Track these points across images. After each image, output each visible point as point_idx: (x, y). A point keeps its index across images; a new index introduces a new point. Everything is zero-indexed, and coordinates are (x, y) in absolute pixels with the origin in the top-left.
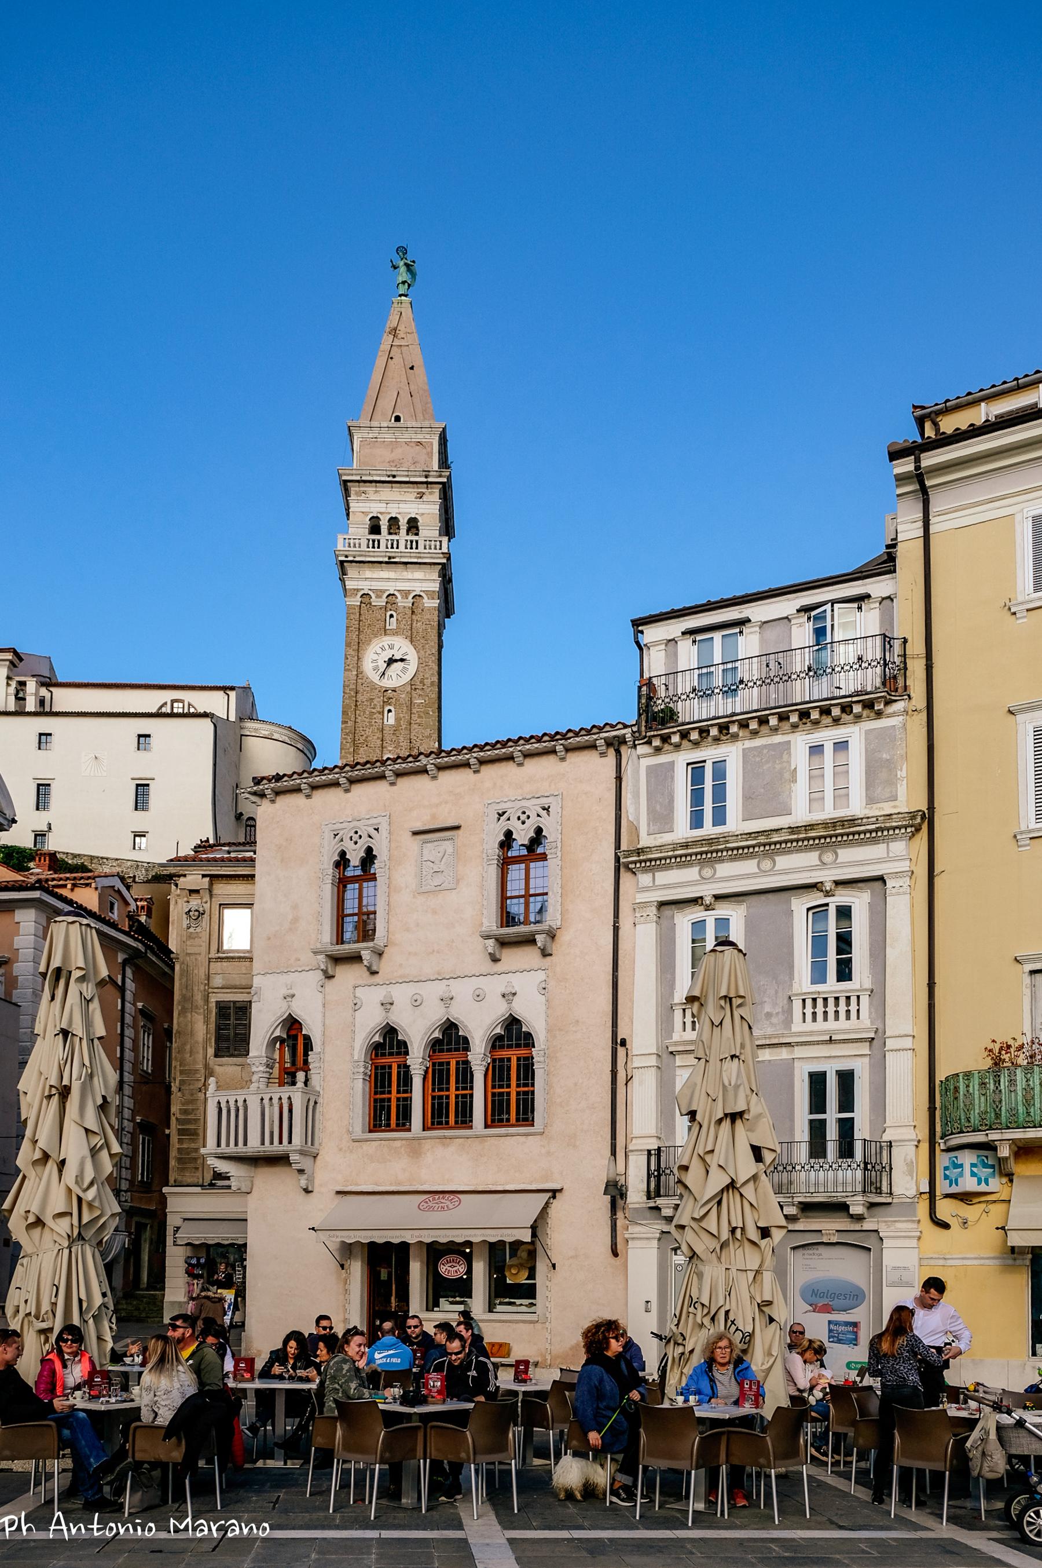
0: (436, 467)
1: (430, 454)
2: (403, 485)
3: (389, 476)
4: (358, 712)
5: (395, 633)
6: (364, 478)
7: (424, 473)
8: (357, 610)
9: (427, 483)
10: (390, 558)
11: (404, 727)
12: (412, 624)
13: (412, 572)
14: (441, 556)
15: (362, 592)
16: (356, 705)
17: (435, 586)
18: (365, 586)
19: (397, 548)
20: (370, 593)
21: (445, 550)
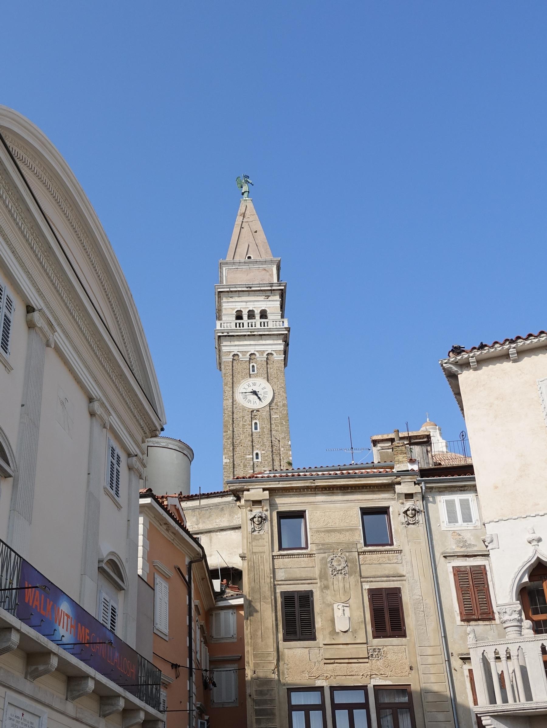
0: (275, 281)
1: (272, 275)
2: (256, 292)
3: (247, 288)
4: (234, 425)
5: (256, 376)
6: (232, 289)
7: (270, 285)
8: (231, 364)
9: (271, 290)
10: (251, 332)
11: (266, 433)
12: (267, 370)
13: (265, 340)
14: (284, 329)
15: (233, 353)
16: (233, 421)
17: (282, 347)
18: (235, 350)
19: (255, 326)
20: (238, 353)
21: (286, 325)
